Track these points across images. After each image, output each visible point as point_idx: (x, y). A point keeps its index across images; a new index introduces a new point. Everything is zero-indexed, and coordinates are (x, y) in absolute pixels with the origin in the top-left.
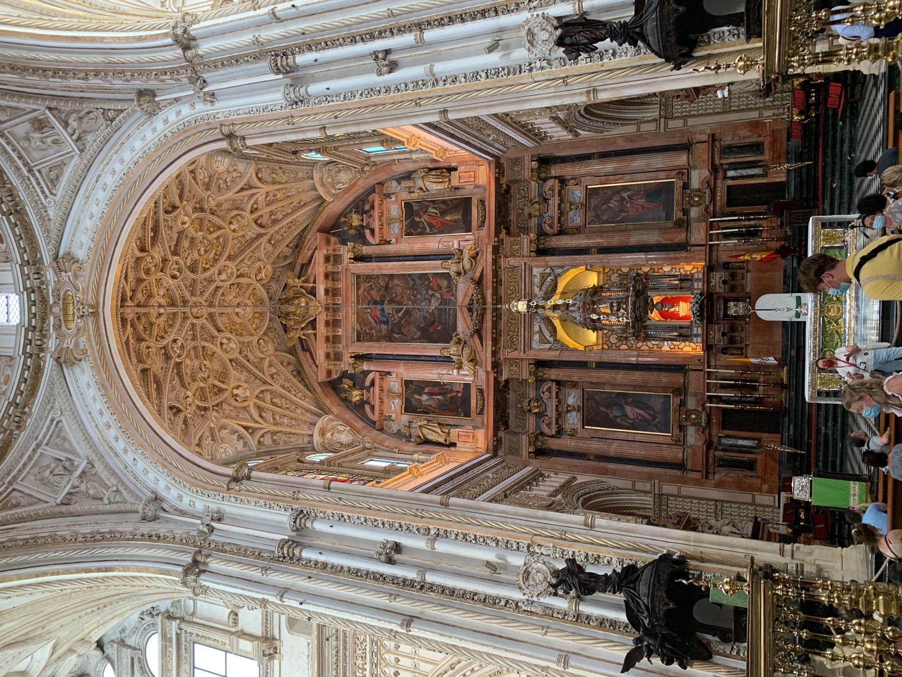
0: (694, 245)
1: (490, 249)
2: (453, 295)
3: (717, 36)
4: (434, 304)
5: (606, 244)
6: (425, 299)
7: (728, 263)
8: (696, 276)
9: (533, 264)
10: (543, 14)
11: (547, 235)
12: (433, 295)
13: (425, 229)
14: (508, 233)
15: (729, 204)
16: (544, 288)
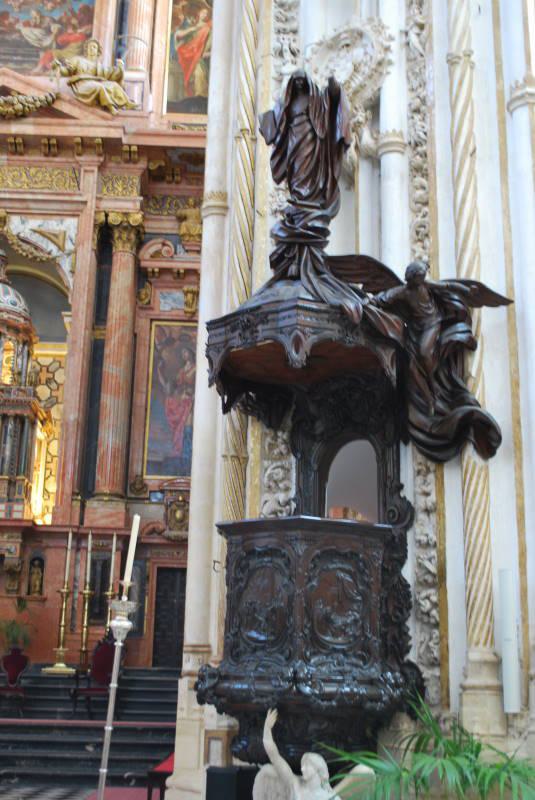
0: (83, 507)
1: (114, 134)
2: (45, 69)
3: (280, 473)
4: (31, 35)
5: (107, 351)
6: (42, 17)
7: (42, 565)
8: (17, 507)
9: (83, 217)
10: (390, 63)
11: (140, 244)
12: (48, 31)
13: (183, 26)
14: (151, 178)
15: (160, 570)
16: (35, 238)
